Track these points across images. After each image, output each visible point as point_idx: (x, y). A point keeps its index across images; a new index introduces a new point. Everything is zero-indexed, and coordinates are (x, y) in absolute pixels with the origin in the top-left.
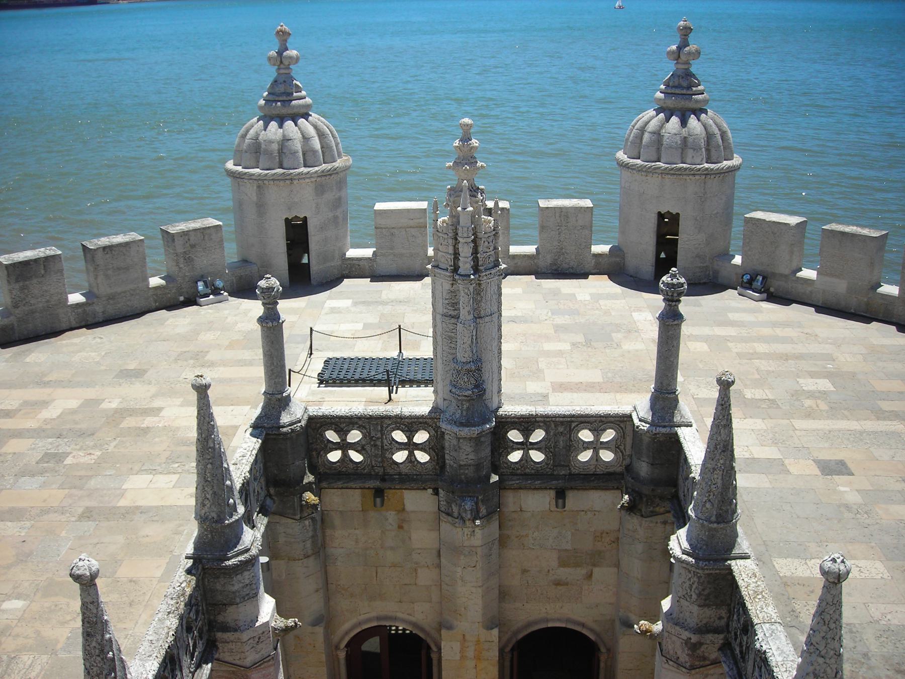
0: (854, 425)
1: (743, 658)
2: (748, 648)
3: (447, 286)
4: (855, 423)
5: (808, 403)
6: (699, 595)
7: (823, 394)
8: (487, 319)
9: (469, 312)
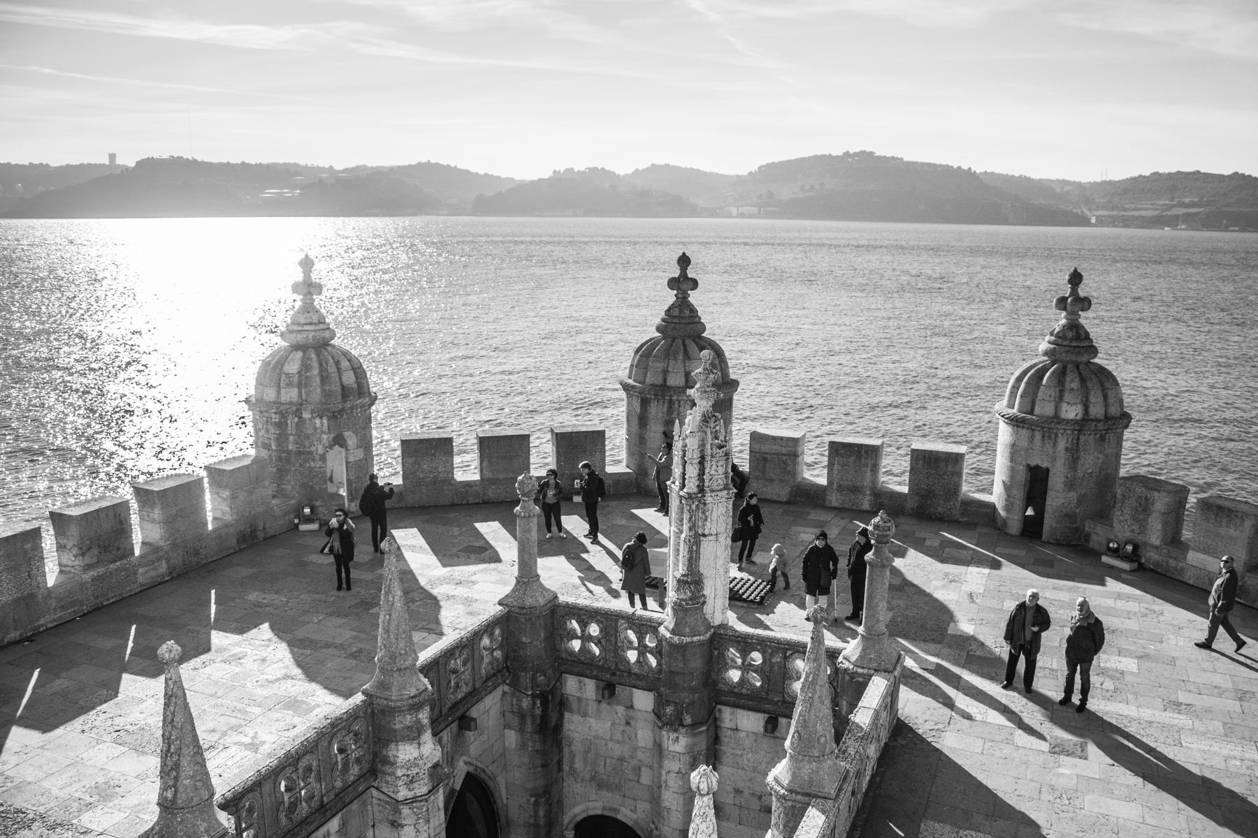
3: (678, 502)
4: (1134, 708)
6: (785, 826)
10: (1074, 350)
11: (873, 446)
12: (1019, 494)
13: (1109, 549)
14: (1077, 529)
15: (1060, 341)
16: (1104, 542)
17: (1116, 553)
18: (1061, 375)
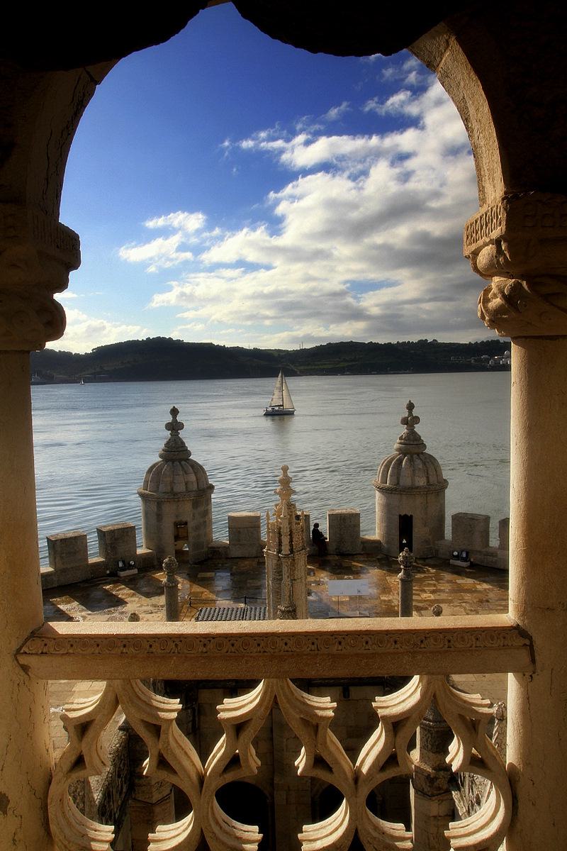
1: (463, 785)
2: (464, 777)
3: (275, 562)
6: (432, 745)
8: (298, 581)
9: (288, 577)
10: (412, 446)
12: (396, 533)
15: (407, 442)
17: (457, 557)
18: (411, 460)
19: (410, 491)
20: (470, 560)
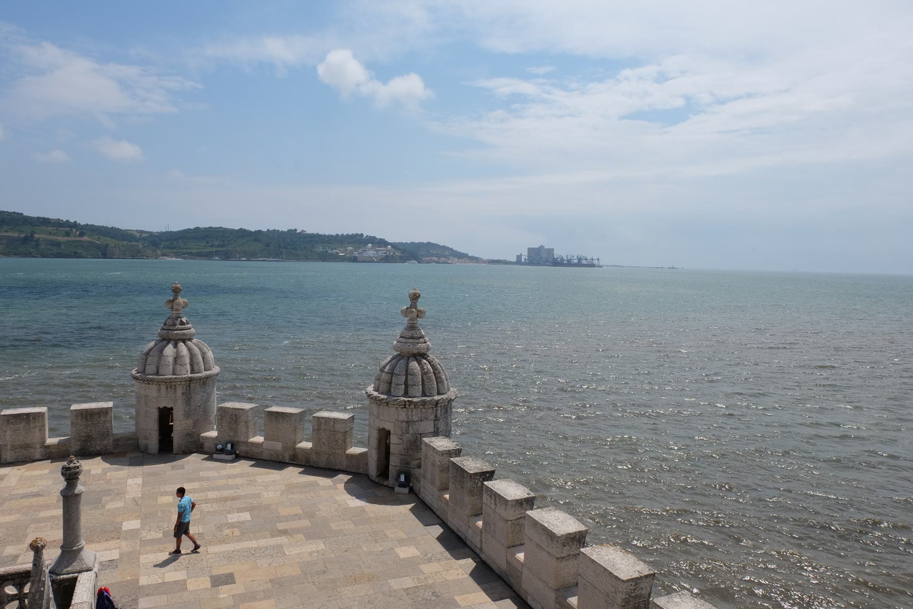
0: (253, 544)
5: (227, 531)
7: (239, 525)
11: (39, 413)
13: (217, 450)
14: (195, 441)
16: (213, 446)
19: (170, 384)
20: (235, 453)
